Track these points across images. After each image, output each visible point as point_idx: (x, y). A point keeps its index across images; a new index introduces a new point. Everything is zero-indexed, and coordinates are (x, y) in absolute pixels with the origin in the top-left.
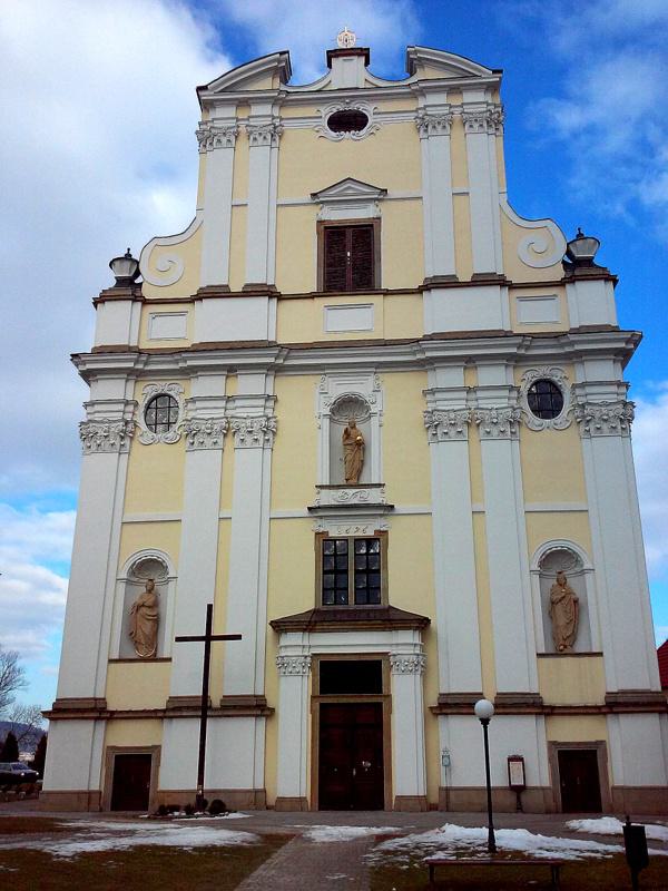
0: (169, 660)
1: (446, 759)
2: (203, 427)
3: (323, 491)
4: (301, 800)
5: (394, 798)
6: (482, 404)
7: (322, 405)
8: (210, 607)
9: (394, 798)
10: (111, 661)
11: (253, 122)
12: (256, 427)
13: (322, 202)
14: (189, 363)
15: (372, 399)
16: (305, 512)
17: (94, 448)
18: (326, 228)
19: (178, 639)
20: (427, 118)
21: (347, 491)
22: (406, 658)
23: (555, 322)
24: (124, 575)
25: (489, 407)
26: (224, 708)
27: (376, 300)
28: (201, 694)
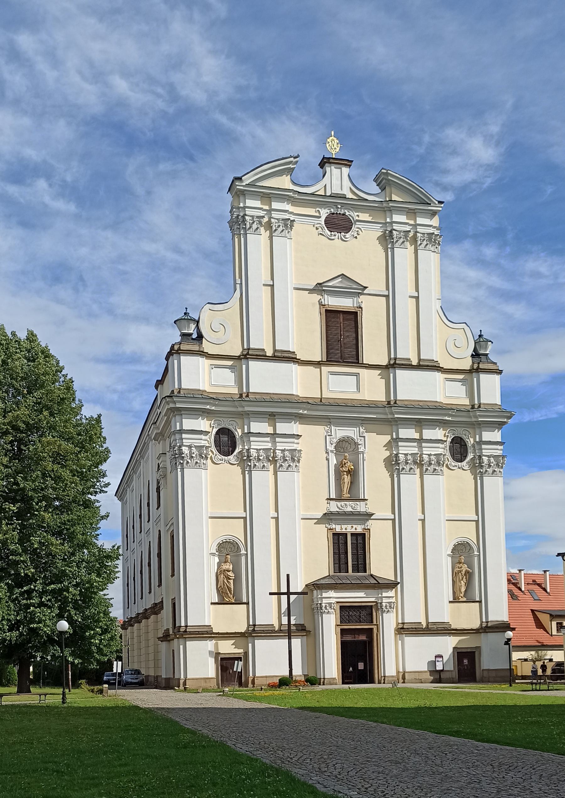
3: (331, 502)
10: (212, 603)
13: (324, 290)
14: (247, 409)
18: (327, 311)
19: (271, 594)
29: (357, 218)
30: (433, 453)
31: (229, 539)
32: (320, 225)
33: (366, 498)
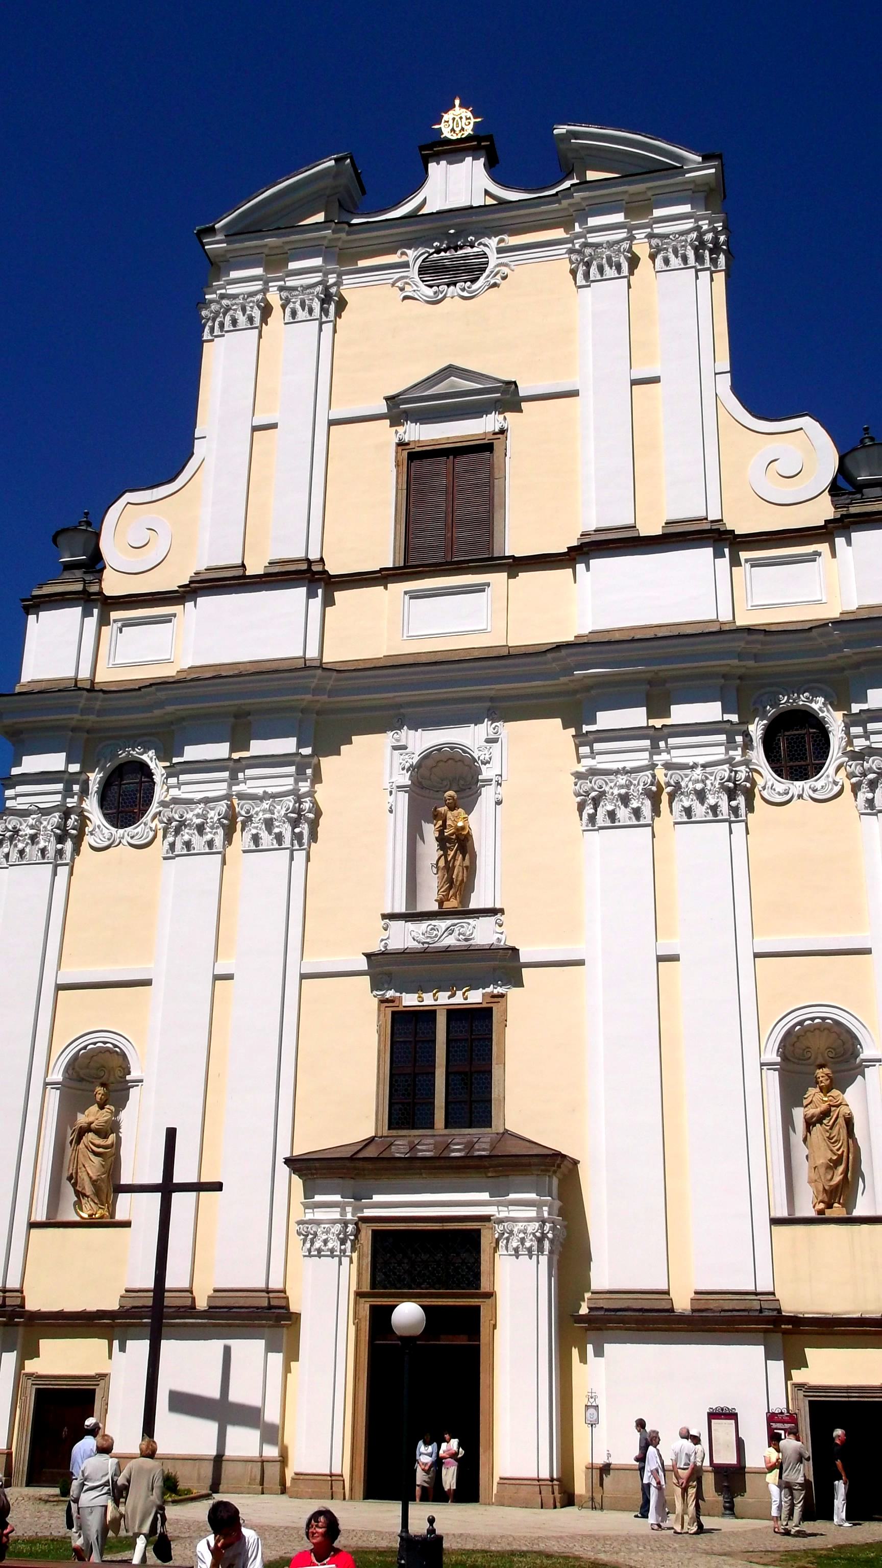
0: (127, 1224)
1: (591, 1411)
2: (189, 816)
4: (333, 1478)
5: (496, 1480)
6: (678, 756)
7: (397, 767)
8: (171, 1134)
9: (496, 1480)
10: (33, 1225)
11: (291, 282)
12: (280, 811)
15: (484, 756)
16: (363, 965)
17: (14, 856)
20: (588, 251)
21: (433, 922)
22: (520, 1226)
23: (818, 602)
24: (57, 1076)
25: (690, 761)
26: (213, 1312)
27: (498, 579)
28: (151, 1285)
29: (502, 245)
30: (701, 760)
31: (95, 1043)
32: (407, 280)
33: (498, 906)
